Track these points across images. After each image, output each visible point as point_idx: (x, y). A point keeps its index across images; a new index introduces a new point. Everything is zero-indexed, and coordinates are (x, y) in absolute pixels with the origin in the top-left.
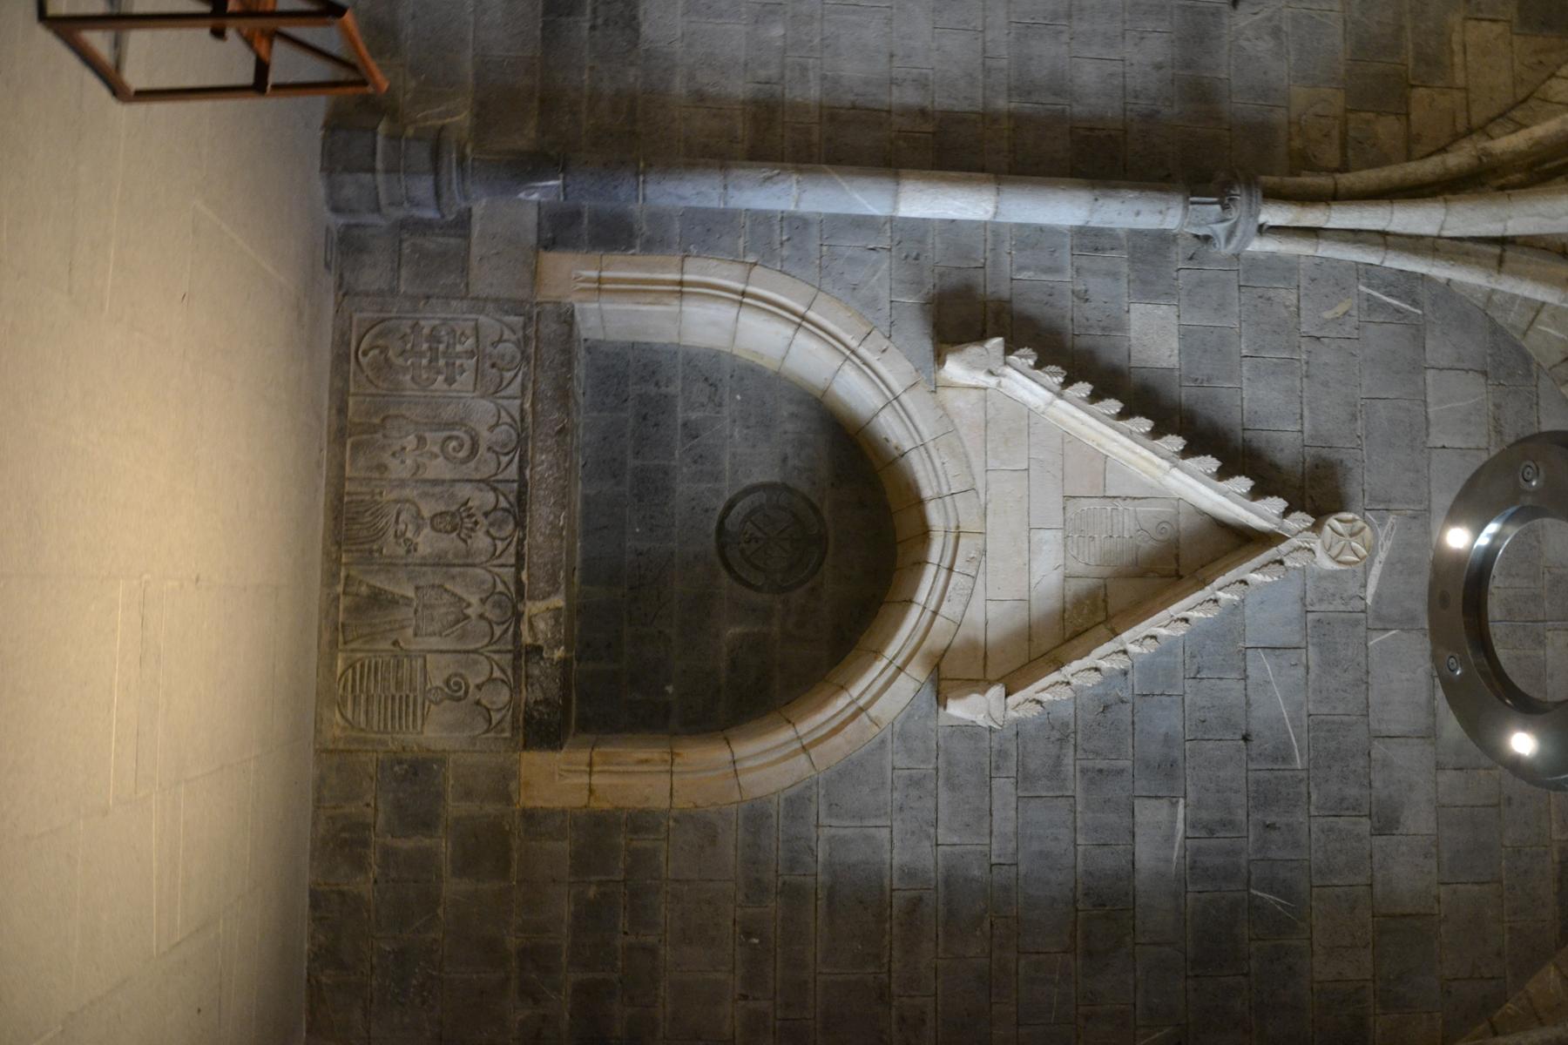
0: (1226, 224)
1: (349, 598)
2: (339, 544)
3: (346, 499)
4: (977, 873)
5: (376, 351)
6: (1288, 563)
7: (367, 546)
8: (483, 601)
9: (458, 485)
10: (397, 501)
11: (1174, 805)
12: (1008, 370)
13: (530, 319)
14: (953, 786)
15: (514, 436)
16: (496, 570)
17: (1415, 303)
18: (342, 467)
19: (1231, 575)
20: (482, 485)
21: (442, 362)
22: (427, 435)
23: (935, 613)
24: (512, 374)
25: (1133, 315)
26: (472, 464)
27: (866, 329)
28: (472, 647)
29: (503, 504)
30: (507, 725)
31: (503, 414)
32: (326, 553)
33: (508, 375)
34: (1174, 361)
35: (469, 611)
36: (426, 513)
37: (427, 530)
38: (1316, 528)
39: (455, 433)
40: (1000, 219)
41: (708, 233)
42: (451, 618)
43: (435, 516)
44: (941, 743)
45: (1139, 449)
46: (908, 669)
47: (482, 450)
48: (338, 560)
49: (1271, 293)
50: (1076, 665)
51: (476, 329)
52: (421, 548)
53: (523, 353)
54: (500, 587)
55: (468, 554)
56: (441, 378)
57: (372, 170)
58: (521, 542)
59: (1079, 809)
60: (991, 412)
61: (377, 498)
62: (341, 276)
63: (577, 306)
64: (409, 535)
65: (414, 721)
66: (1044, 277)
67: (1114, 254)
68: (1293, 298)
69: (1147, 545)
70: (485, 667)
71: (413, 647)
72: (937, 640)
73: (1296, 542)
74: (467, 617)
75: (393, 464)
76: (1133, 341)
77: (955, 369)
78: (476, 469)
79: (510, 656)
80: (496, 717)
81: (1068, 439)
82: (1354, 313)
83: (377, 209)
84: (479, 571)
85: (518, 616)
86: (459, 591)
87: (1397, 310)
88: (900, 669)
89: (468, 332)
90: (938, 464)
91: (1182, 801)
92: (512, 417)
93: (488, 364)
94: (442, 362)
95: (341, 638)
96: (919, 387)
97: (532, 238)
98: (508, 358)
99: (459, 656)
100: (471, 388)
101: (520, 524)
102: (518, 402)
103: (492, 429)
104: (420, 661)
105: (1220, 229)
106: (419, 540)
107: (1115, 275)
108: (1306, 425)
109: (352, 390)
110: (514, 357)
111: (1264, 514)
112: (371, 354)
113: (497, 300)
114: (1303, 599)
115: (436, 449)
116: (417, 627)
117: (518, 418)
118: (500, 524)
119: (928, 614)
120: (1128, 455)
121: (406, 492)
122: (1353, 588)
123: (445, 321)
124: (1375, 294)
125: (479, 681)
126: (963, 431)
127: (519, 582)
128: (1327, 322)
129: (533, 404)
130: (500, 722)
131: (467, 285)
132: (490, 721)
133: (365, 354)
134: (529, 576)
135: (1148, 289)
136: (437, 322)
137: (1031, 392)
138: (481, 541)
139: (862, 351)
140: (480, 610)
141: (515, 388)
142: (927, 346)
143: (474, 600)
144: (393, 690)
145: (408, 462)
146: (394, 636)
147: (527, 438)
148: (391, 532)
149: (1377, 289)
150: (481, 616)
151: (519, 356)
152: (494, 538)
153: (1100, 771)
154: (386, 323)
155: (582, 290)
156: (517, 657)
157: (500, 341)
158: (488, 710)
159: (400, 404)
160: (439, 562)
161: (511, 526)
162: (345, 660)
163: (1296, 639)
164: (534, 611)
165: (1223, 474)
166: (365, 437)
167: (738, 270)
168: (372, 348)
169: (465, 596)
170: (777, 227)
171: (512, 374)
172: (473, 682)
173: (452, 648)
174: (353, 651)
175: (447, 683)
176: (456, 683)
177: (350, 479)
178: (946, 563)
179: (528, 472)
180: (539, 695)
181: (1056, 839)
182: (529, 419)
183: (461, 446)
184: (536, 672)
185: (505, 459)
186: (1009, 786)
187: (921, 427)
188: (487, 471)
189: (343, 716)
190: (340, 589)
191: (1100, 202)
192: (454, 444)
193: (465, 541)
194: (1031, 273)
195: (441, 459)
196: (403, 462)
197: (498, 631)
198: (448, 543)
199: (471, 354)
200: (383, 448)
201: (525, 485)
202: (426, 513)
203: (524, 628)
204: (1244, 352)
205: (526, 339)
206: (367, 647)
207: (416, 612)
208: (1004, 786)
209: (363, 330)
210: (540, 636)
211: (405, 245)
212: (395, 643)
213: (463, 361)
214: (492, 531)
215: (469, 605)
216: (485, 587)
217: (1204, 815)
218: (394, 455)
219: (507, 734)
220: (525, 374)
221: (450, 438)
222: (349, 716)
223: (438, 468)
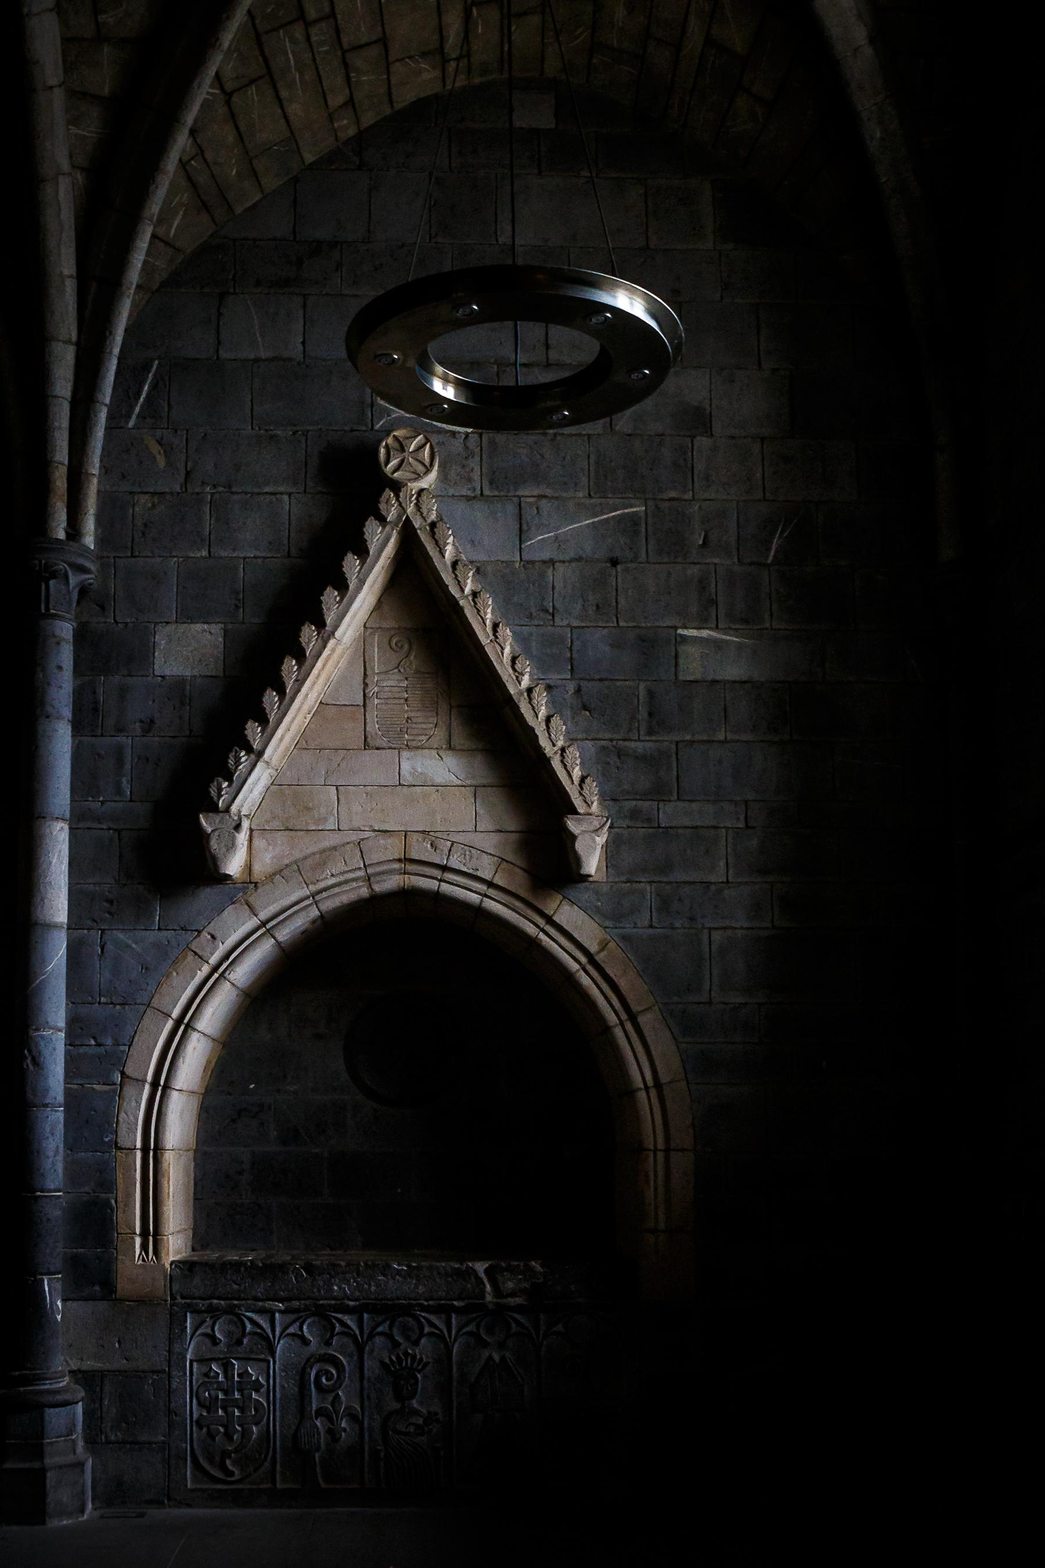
0: (70, 574)
4: (755, 842)
5: (228, 1462)
6: (433, 517)
8: (485, 1345)
11: (684, 639)
12: (234, 808)
13: (189, 1305)
14: (666, 867)
17: (147, 368)
19: (447, 578)
23: (490, 884)
25: (168, 673)
27: (190, 957)
31: (291, 1330)
33: (249, 1327)
34: (216, 629)
36: (396, 1406)
37: (415, 1403)
38: (396, 487)
40: (68, 815)
41: (92, 1122)
44: (624, 879)
45: (315, 671)
46: (549, 912)
49: (139, 523)
50: (544, 742)
57: (43, 1471)
59: (688, 737)
60: (276, 824)
63: (172, 1259)
64: (420, 1421)
66: (128, 766)
67: (100, 691)
68: (143, 499)
69: (414, 662)
72: (518, 882)
73: (410, 509)
74: (503, 1359)
76: (196, 673)
77: (234, 866)
78: (351, 1356)
81: (303, 743)
82: (159, 433)
83: (81, 1465)
87: (154, 387)
88: (550, 920)
89: (205, 1369)
90: (332, 881)
91: (680, 631)
96: (251, 900)
97: (103, 1306)
98: (232, 1328)
100: (264, 1365)
103: (305, 1342)
105: (74, 580)
106: (424, 1411)
107: (123, 692)
108: (281, 489)
109: (269, 1485)
110: (230, 1322)
111: (383, 545)
112: (231, 1468)
114: (468, 499)
115: (330, 1397)
117: (293, 1317)
119: (491, 892)
120: (321, 681)
122: (457, 445)
123: (195, 1394)
124: (137, 409)
126: (298, 855)
128: (169, 464)
131: (154, 1372)
133: (232, 1474)
135: (139, 655)
137: (255, 784)
139: (213, 960)
142: (207, 895)
143: (486, 1354)
147: (316, 1306)
149: (131, 408)
153: (650, 714)
154: (198, 1452)
155: (156, 1252)
163: (511, 508)
165: (342, 585)
166: (318, 1470)
167: (129, 1090)
169: (483, 1362)
170: (82, 1050)
178: (437, 873)
181: (720, 762)
182: (296, 1304)
185: (338, 1328)
186: (669, 808)
187: (293, 898)
188: (352, 1347)
191: (49, 709)
194: (124, 780)
199: (227, 1367)
202: (396, 1406)
203: (512, 1301)
204: (204, 553)
208: (669, 813)
211: (113, 1438)
214: (414, 1337)
215: (490, 1358)
217: (694, 609)
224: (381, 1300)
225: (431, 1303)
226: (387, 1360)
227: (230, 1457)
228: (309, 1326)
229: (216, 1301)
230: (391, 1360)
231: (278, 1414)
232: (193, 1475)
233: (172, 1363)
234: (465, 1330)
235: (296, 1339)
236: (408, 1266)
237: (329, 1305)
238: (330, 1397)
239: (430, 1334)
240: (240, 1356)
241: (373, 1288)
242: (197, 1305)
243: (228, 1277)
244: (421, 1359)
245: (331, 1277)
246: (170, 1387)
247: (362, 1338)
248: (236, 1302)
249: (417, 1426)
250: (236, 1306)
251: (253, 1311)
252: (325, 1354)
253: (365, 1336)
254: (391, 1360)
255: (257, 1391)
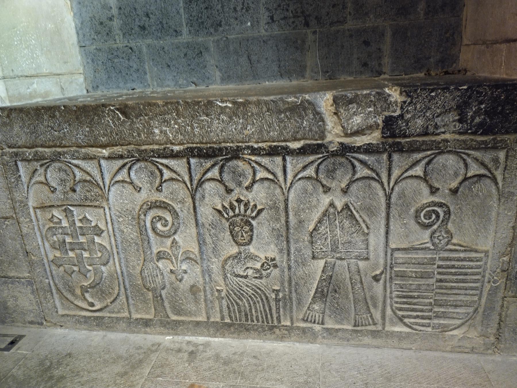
1: (327, 319)
2: (272, 328)
3: (227, 320)
5: (87, 295)
7: (273, 304)
8: (327, 190)
9: (201, 220)
10: (225, 277)
13: (16, 154)
15: (142, 164)
16: (290, 177)
18: (198, 323)
20: (198, 196)
21: (82, 239)
22: (155, 251)
24: (76, 171)
26: (177, 207)
28: (383, 200)
29: (215, 173)
30: (487, 157)
31: (119, 177)
32: (282, 338)
35: (339, 205)
36: (234, 250)
37: (252, 249)
39: (148, 225)
42: (347, 223)
43: (236, 243)
47: (161, 197)
48: (290, 329)
51: (43, 208)
52: (270, 255)
53: (53, 161)
54: (310, 172)
55: (274, 207)
56: (97, 239)
58: (255, 151)
61: (223, 294)
62: (32, 323)
64: (258, 266)
65: (471, 260)
70: (410, 185)
71: (382, 261)
74: (346, 207)
75: (188, 280)
78: (182, 202)
79: (396, 157)
80: (475, 169)
84: (292, 196)
85: (345, 150)
86: (316, 216)
92: (120, 169)
93: (75, 196)
94: (82, 239)
95: (372, 328)
98: (63, 175)
99: (394, 212)
101: (235, 154)
102: (102, 162)
104: (397, 255)
106: (262, 256)
109: (126, 314)
110: (60, 169)
112: (90, 300)
113: (10, 190)
115: (169, 242)
116: (357, 258)
117: (121, 162)
118: (238, 176)
121: (215, 266)
125: (425, 190)
127: (303, 151)
129: (104, 146)
130: (483, 164)
132: (480, 176)
133: (92, 305)
134: (295, 139)
136: (47, 245)
138: (259, 195)
140: (338, 193)
141: (89, 166)
143: (326, 200)
144: (432, 281)
145: (184, 267)
146: (367, 280)
147: (140, 152)
148: (257, 282)
150: (345, 191)
151: (57, 165)
152: (254, 182)
154: (61, 286)
156: (400, 149)
157: (47, 184)
158: (465, 179)
159: (130, 275)
160: (285, 236)
161: (240, 163)
162: (393, 324)
164: (338, 130)
166: (166, 304)
168: (85, 299)
169: (322, 209)
171: (76, 171)
172: (426, 198)
173: (383, 222)
174: (383, 317)
175: (426, 226)
176: (428, 216)
177: (208, 318)
179: (176, 148)
180: (453, 116)
182: (118, 150)
183: (160, 218)
184: (420, 122)
185: (167, 174)
188: (183, 193)
189: (459, 327)
190: (317, 327)
192: (159, 226)
193: (260, 212)
195: (176, 237)
196: (185, 272)
197: (362, 172)
198: (262, 228)
200: (175, 289)
201: (192, 149)
202: (234, 250)
205: (38, 158)
206: (380, 305)
207: (341, 259)
209: (72, 306)
210: (371, 121)
212: (376, 279)
213: (76, 219)
214: (247, 184)
215: (332, 205)
216: (310, 188)
218: (181, 281)
219: (502, 155)
220: (73, 157)
221: (154, 229)
222: (458, 322)
223: (186, 239)
224: (206, 143)
225: (260, 145)
226: (219, 207)
227: (87, 292)
228: (136, 172)
229: (40, 149)
230: (223, 206)
231: (122, 256)
232: (62, 304)
233: (17, 211)
234: (300, 176)
235: (126, 185)
236: (234, 103)
237: (153, 151)
238: (169, 242)
239: (262, 180)
240: (76, 203)
241: (197, 130)
242: (23, 153)
243: (46, 123)
244: (255, 206)
245: (150, 119)
246: (21, 232)
247: (191, 185)
248: (59, 150)
249: (257, 271)
250: (60, 153)
251: (78, 158)
252: (156, 201)
253: (195, 182)
254: (223, 206)
255: (99, 235)
